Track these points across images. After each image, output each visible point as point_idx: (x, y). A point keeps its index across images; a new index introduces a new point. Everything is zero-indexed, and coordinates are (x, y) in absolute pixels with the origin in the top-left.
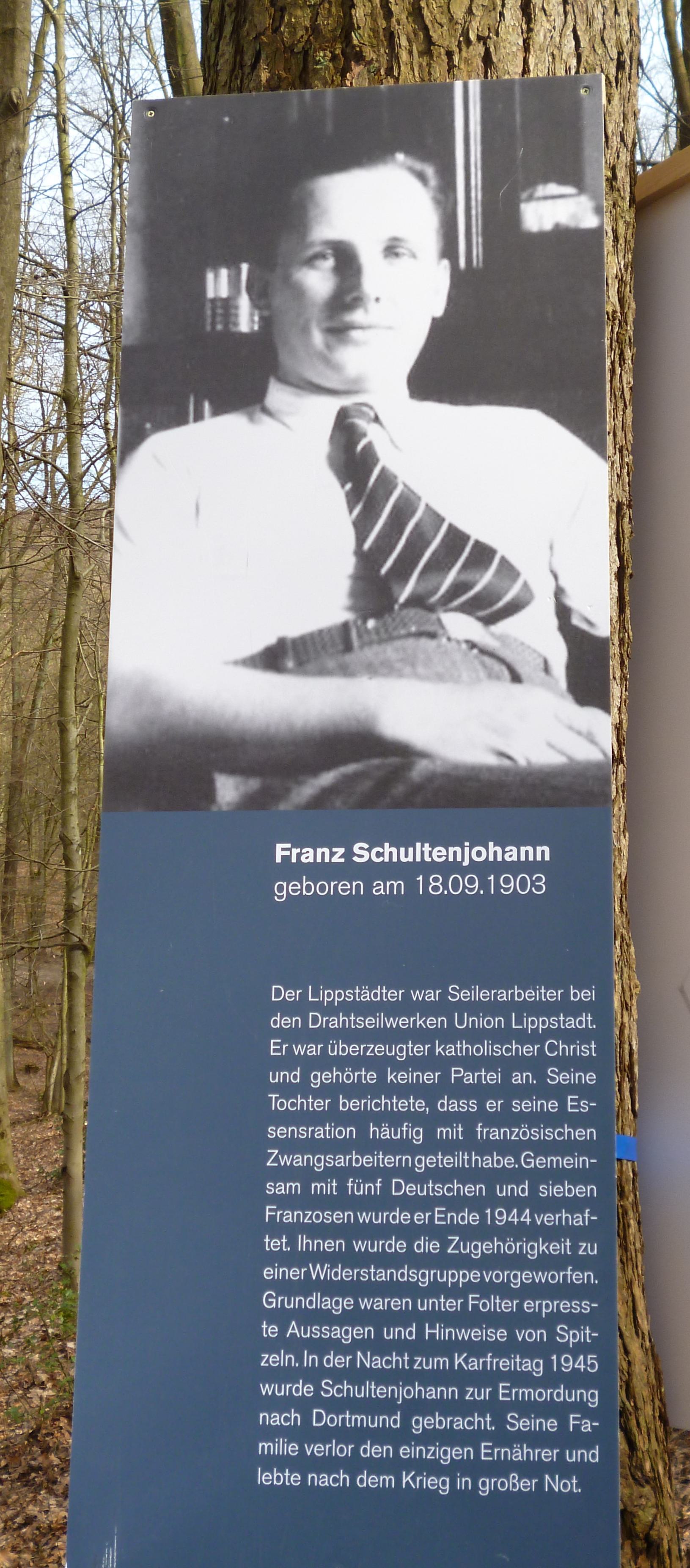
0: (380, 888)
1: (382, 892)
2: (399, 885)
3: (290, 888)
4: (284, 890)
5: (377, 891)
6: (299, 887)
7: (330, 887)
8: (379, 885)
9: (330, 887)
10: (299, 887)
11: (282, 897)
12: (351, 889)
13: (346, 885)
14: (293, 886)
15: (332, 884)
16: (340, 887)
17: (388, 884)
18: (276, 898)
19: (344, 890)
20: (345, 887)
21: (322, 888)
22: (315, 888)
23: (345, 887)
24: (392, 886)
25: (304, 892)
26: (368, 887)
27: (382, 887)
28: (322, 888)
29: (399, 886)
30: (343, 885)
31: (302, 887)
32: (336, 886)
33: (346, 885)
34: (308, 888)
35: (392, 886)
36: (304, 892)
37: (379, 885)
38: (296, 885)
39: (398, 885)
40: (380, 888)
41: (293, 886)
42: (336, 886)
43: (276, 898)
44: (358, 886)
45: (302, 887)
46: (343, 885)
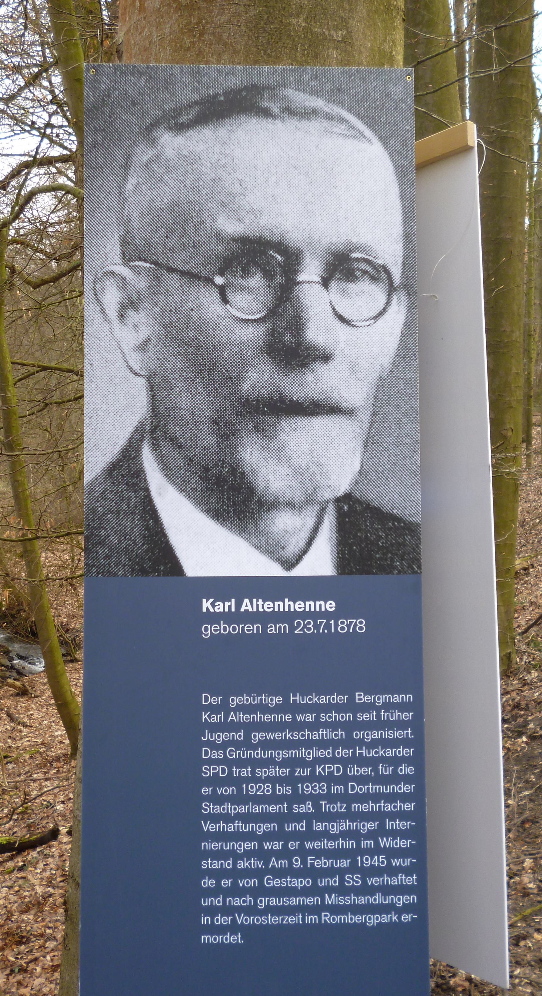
0: (272, 629)
3: (213, 629)
5: (270, 631)
7: (239, 629)
8: (271, 627)
9: (239, 629)
10: (219, 628)
11: (207, 635)
12: (253, 630)
13: (250, 627)
16: (246, 629)
17: (278, 626)
19: (248, 630)
20: (250, 629)
21: (234, 629)
22: (230, 629)
23: (250, 629)
24: (280, 627)
25: (222, 632)
26: (265, 629)
27: (274, 628)
28: (234, 629)
29: (285, 627)
30: (248, 627)
31: (222, 628)
32: (243, 628)
34: (225, 629)
35: (280, 627)
36: (222, 632)
37: (272, 627)
39: (284, 627)
40: (272, 629)
42: (243, 628)
44: (258, 627)
46: (248, 627)
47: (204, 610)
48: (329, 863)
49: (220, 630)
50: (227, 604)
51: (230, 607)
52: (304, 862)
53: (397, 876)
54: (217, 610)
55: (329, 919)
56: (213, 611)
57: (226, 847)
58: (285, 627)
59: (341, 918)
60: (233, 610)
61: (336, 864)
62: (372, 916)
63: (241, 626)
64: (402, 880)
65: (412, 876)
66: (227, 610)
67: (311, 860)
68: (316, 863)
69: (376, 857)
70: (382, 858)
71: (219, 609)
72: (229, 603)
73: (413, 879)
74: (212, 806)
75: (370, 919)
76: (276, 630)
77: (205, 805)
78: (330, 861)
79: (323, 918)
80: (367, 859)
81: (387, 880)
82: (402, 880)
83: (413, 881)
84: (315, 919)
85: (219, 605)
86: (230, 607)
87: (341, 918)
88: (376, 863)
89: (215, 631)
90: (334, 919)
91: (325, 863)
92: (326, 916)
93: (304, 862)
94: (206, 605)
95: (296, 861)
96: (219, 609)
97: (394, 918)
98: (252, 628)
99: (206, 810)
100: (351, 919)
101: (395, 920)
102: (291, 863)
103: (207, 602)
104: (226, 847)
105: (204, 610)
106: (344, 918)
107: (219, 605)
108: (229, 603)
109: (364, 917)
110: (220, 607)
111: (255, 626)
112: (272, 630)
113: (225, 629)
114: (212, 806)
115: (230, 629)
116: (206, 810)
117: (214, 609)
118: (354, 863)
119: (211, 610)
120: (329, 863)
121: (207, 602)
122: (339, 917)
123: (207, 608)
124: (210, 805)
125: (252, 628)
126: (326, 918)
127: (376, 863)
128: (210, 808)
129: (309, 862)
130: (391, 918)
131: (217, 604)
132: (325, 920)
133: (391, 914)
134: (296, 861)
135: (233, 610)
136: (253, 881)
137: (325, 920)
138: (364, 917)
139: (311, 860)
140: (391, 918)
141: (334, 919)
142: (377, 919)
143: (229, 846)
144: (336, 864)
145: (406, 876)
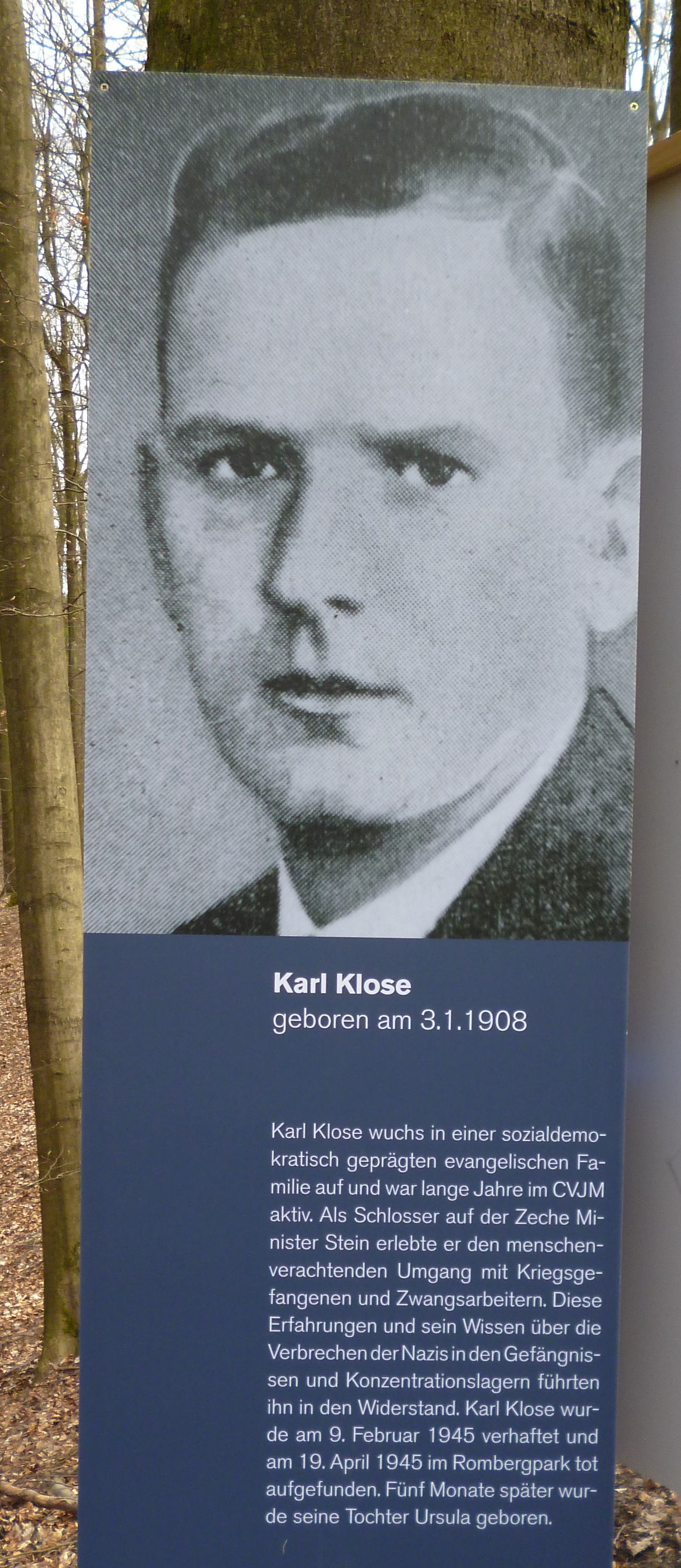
0: (386, 1023)
1: (388, 1026)
2: (406, 1019)
3: (290, 1020)
4: (284, 1023)
5: (382, 1025)
6: (300, 1020)
7: (332, 1021)
9: (332, 1021)
10: (300, 1020)
12: (355, 1023)
13: (350, 1018)
14: (293, 1018)
15: (335, 1017)
16: (343, 1021)
17: (394, 1018)
18: (275, 1030)
20: (349, 1021)
22: (317, 1021)
23: (349, 1021)
24: (398, 1020)
25: (305, 1025)
26: (374, 1021)
27: (388, 1021)
29: (406, 1020)
30: (346, 1018)
31: (305, 1019)
32: (339, 1019)
33: (350, 1018)
34: (310, 1021)
35: (398, 1020)
36: (305, 1025)
38: (297, 1018)
39: (404, 1020)
40: (386, 1023)
41: (293, 1018)
42: (339, 1019)
43: (275, 1030)
44: (362, 1019)
45: (305, 1019)
46: (346, 1018)
47: (277, 990)
48: (386, 1436)
49: (302, 1022)
50: (314, 981)
51: (318, 986)
52: (347, 1434)
53: (529, 1431)
54: (298, 991)
55: (464, 1464)
56: (291, 992)
57: (328, 1328)
58: (406, 1020)
59: (482, 1463)
60: (324, 990)
61: (397, 1438)
62: (530, 1462)
63: (335, 1017)
64: (536, 1436)
65: (552, 1432)
66: (313, 991)
67: (358, 1431)
68: (365, 1436)
69: (459, 1429)
70: (468, 1431)
71: (300, 988)
72: (318, 980)
73: (554, 1436)
74: (340, 1240)
75: (526, 1465)
76: (391, 1025)
77: (330, 1238)
78: (387, 1434)
79: (455, 1462)
80: (444, 1432)
81: (514, 1436)
82: (536, 1436)
83: (553, 1439)
84: (443, 1463)
85: (301, 982)
86: (318, 986)
87: (482, 1463)
88: (459, 1438)
89: (294, 1023)
90: (471, 1464)
91: (380, 1436)
92: (459, 1459)
93: (347, 1434)
94: (280, 982)
95: (335, 1432)
96: (300, 988)
97: (564, 1465)
98: (353, 1020)
99: (331, 1245)
100: (498, 1465)
101: (565, 1468)
102: (326, 1435)
103: (281, 977)
104: (328, 1328)
105: (277, 990)
106: (488, 1463)
107: (301, 982)
108: (318, 980)
109: (517, 1462)
110: (302, 986)
111: (358, 1017)
112: (385, 1024)
113: (310, 1021)
114: (340, 1240)
115: (317, 1021)
116: (331, 1245)
117: (293, 988)
118: (424, 1437)
119: (289, 990)
120: (386, 1436)
121: (281, 977)
122: (479, 1462)
123: (282, 987)
124: (338, 1238)
125: (353, 1020)
126: (460, 1463)
127: (459, 1438)
128: (338, 1243)
129: (355, 1434)
130: (559, 1464)
131: (297, 980)
132: (457, 1465)
133: (559, 1458)
134: (335, 1432)
135: (324, 990)
136: (373, 1379)
137: (457, 1465)
138: (517, 1462)
139: (358, 1431)
140: (559, 1464)
141: (471, 1464)
142: (538, 1465)
143: (333, 1327)
144: (397, 1438)
145: (543, 1432)
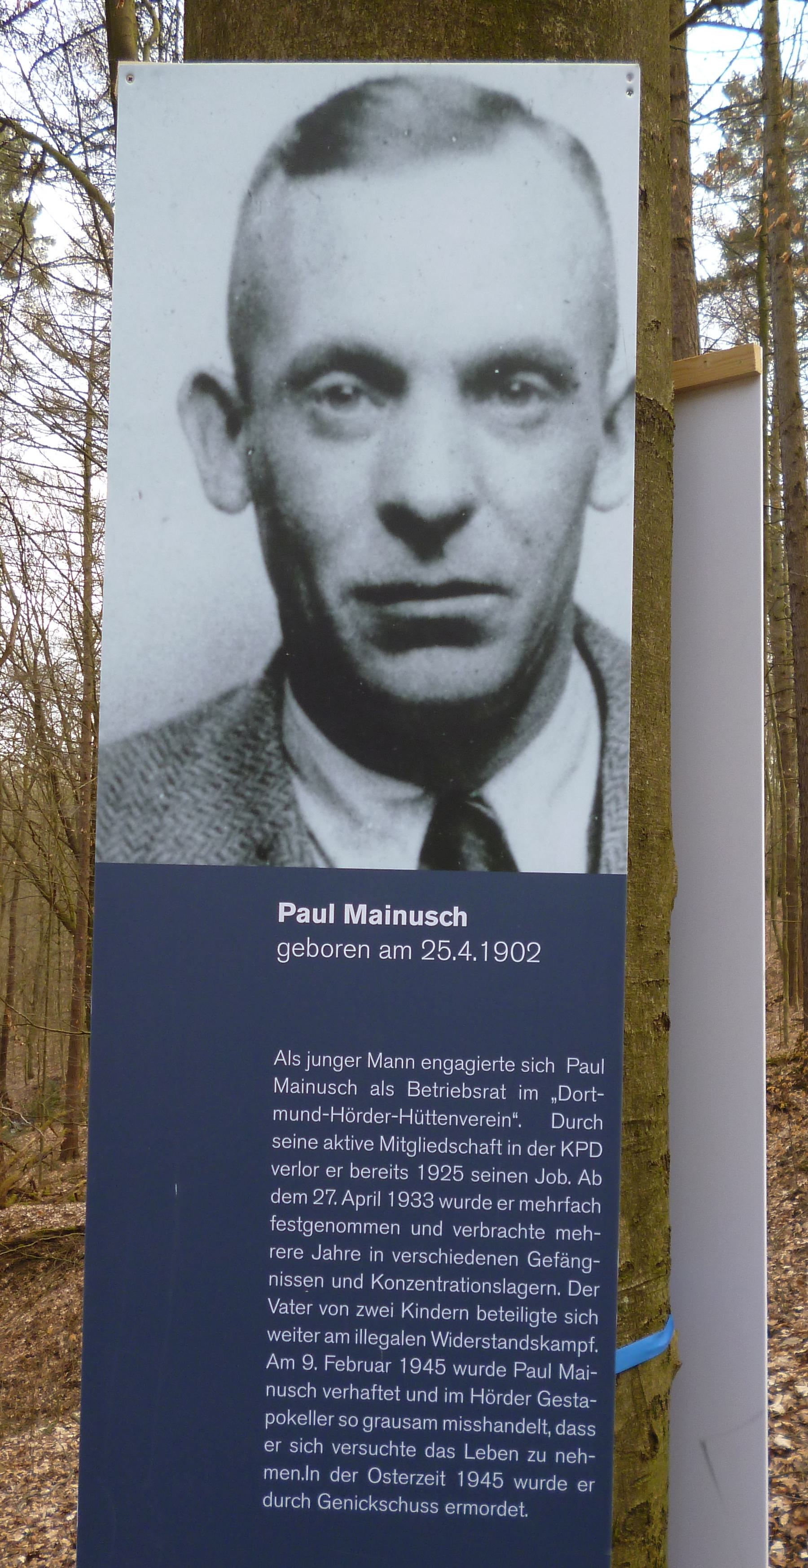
5: (383, 955)
20: (351, 950)
22: (319, 950)
23: (351, 950)
26: (375, 951)
27: (389, 951)
31: (308, 949)
32: (341, 949)
34: (313, 950)
35: (399, 950)
40: (387, 952)
42: (341, 949)
48: (357, 1365)
52: (319, 1362)
61: (368, 1368)
63: (337, 946)
67: (329, 1359)
71: (303, 918)
91: (351, 1366)
93: (319, 1362)
95: (308, 1359)
96: (303, 918)
102: (299, 1364)
120: (357, 1365)
129: (326, 1362)
134: (308, 1359)
139: (329, 1359)
144: (368, 1368)
